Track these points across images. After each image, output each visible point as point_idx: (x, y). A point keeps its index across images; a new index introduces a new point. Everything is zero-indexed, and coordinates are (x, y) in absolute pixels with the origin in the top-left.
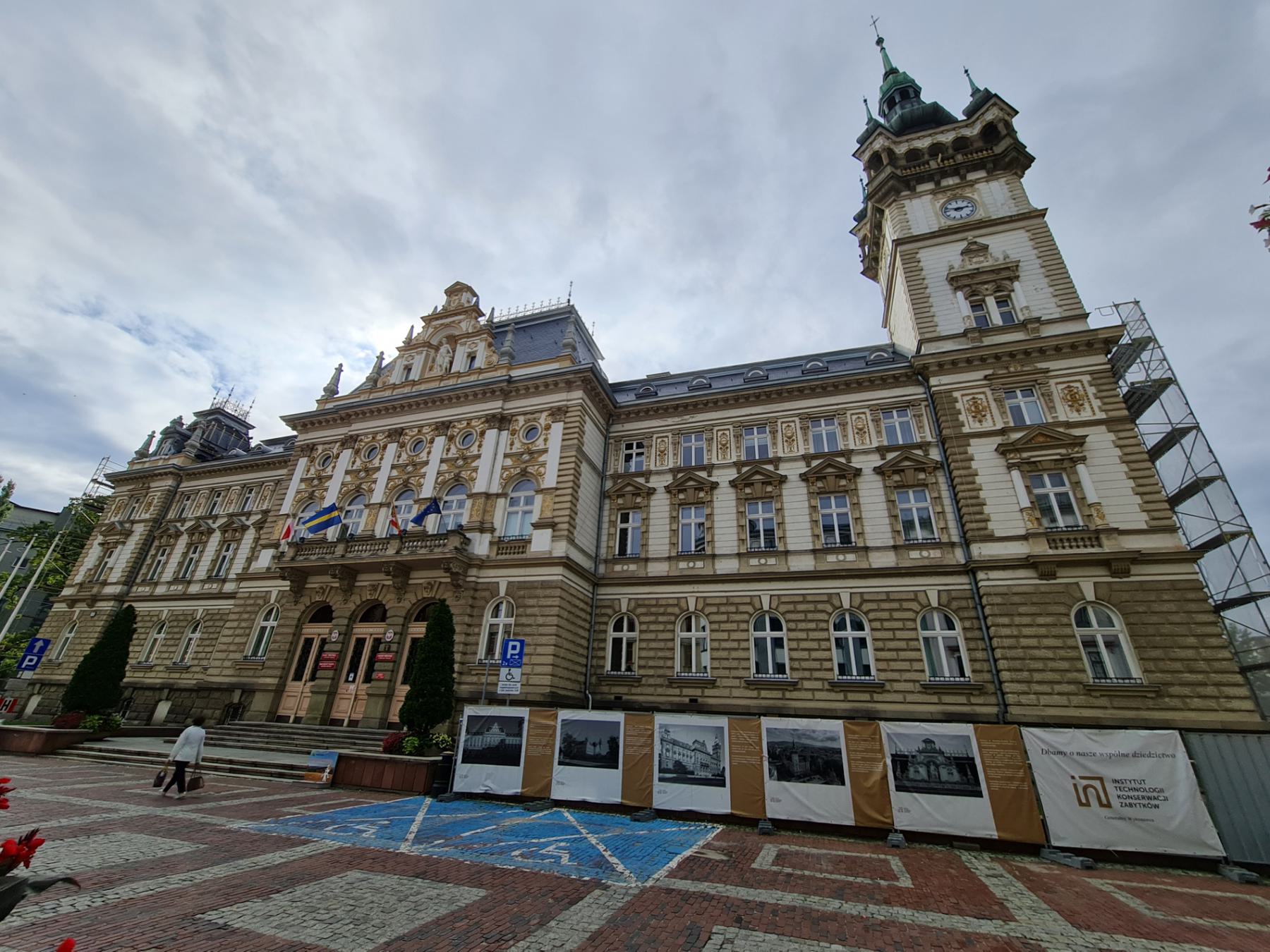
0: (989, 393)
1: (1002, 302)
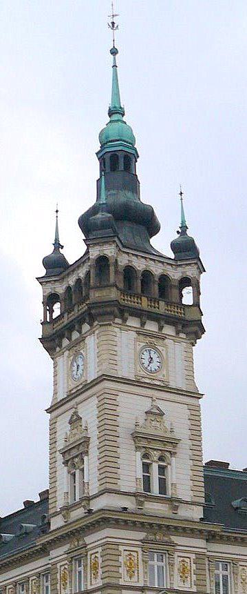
0: (140, 553)
1: (162, 470)
